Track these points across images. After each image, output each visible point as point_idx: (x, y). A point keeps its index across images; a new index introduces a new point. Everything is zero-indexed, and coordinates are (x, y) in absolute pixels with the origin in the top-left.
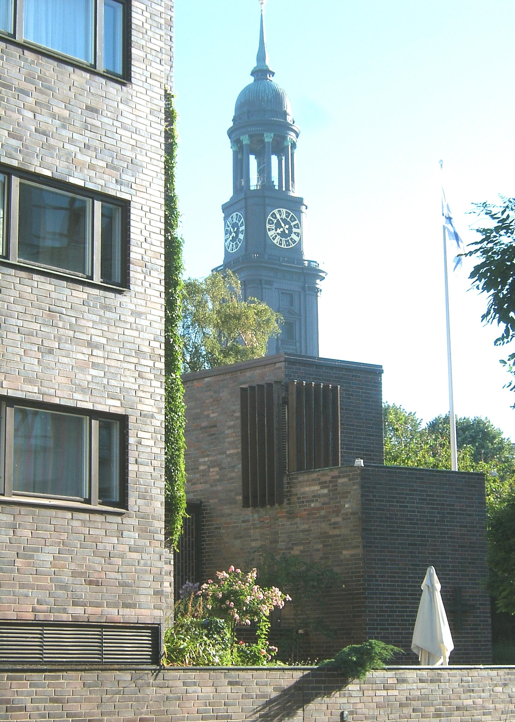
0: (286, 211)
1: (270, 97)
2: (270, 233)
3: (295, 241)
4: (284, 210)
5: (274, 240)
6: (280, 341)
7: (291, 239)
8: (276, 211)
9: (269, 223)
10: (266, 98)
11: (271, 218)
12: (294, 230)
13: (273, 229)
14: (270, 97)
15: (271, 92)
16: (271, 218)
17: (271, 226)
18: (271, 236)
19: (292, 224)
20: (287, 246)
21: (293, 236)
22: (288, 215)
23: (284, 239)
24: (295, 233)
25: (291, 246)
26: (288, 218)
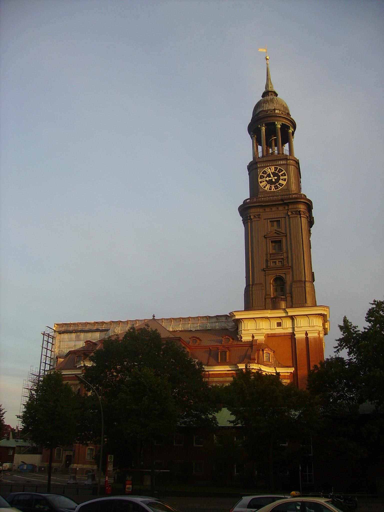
2: (261, 185)
5: (265, 188)
6: (269, 255)
7: (280, 184)
9: (261, 178)
11: (263, 175)
12: (281, 177)
13: (263, 181)
16: (263, 175)
17: (262, 179)
18: (262, 186)
19: (280, 174)
20: (275, 189)
21: (281, 182)
23: (273, 185)
24: (282, 179)
25: (279, 189)
26: (276, 171)
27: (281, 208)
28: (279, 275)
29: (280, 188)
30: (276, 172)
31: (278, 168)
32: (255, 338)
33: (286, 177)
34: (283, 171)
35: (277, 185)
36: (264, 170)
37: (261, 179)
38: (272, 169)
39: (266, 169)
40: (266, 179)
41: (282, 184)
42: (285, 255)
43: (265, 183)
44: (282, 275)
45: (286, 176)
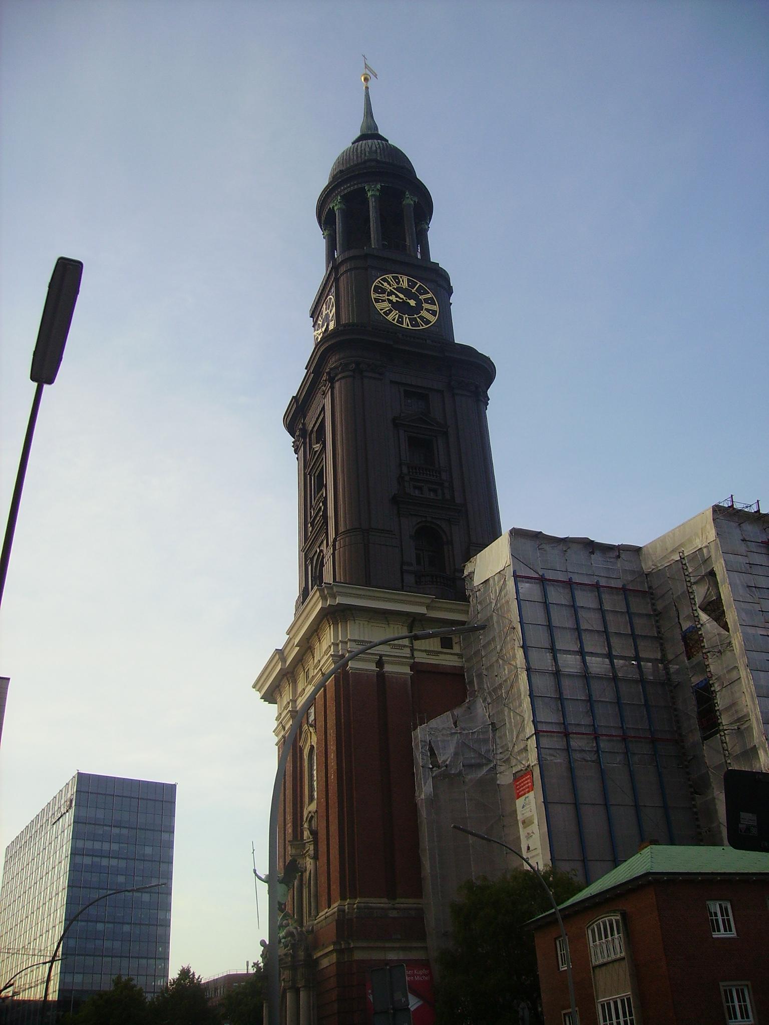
0: (408, 279)
1: (374, 148)
2: (378, 306)
3: (428, 322)
4: (405, 278)
7: (422, 318)
8: (389, 277)
9: (376, 291)
13: (383, 301)
14: (374, 148)
17: (381, 295)
18: (381, 310)
22: (412, 284)
23: (406, 316)
26: (413, 289)
29: (423, 326)
30: (413, 291)
32: (388, 668)
33: (436, 308)
34: (429, 293)
35: (415, 318)
36: (384, 278)
37: (378, 294)
38: (403, 281)
39: (388, 277)
40: (390, 298)
42: (444, 476)
43: (386, 306)
45: (436, 305)
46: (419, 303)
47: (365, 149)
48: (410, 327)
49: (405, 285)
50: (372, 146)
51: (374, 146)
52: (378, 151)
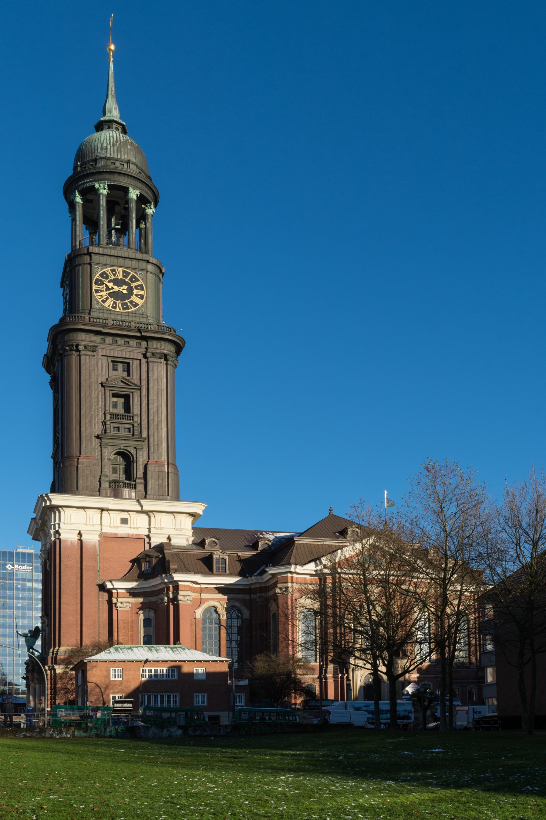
3: (136, 305)
4: (121, 270)
7: (131, 302)
10: (99, 146)
12: (135, 292)
14: (105, 145)
15: (108, 138)
19: (133, 285)
21: (134, 298)
22: (126, 274)
23: (120, 301)
24: (137, 295)
25: (130, 310)
26: (126, 278)
27: (133, 342)
28: (126, 448)
29: (132, 308)
30: (126, 281)
31: (130, 273)
34: (139, 280)
35: (127, 303)
41: (135, 303)
44: (129, 449)
46: (130, 290)
47: (97, 145)
48: (122, 310)
49: (120, 276)
50: (103, 142)
51: (105, 141)
52: (109, 147)
